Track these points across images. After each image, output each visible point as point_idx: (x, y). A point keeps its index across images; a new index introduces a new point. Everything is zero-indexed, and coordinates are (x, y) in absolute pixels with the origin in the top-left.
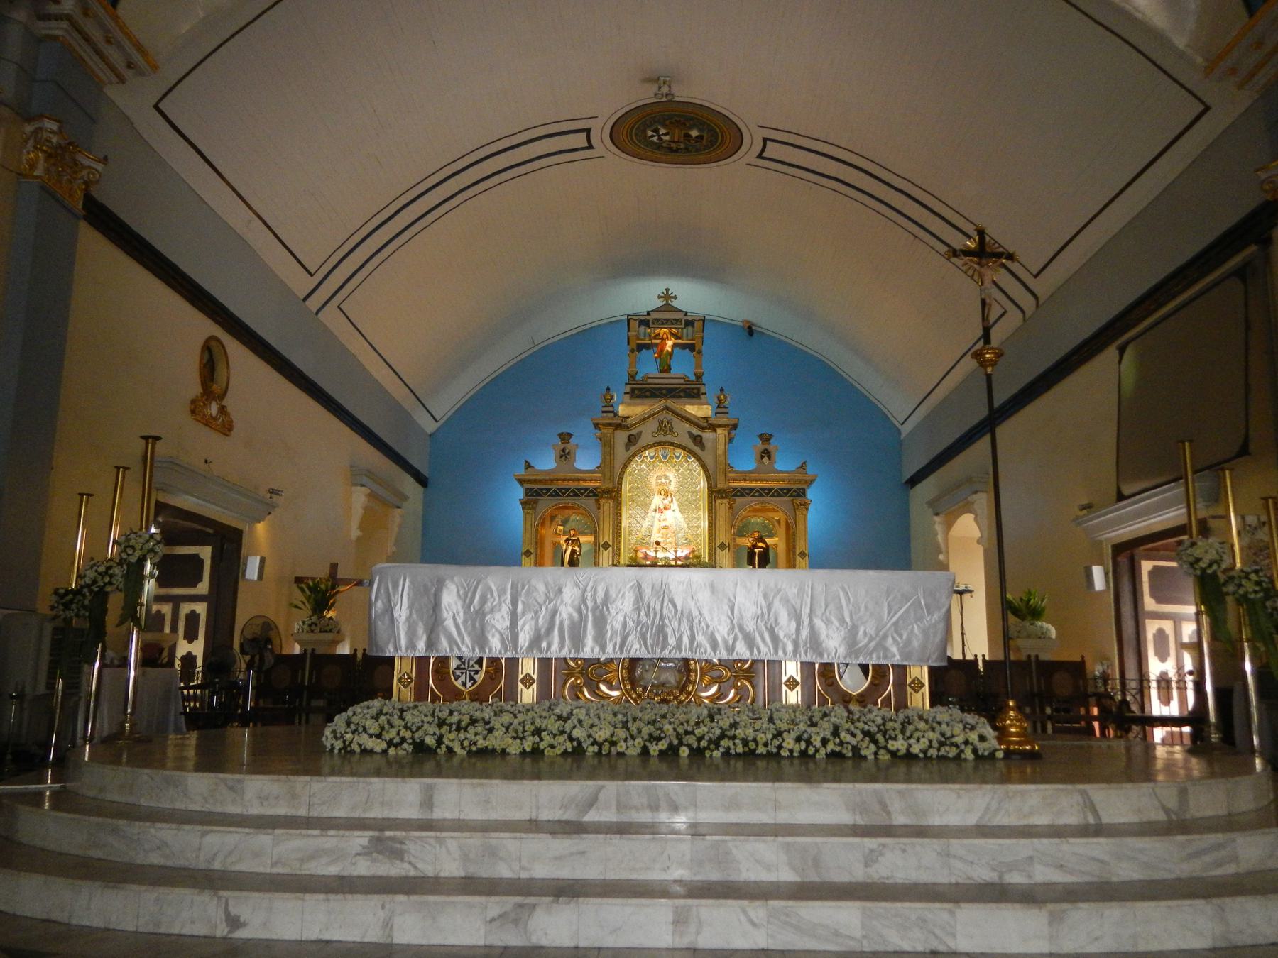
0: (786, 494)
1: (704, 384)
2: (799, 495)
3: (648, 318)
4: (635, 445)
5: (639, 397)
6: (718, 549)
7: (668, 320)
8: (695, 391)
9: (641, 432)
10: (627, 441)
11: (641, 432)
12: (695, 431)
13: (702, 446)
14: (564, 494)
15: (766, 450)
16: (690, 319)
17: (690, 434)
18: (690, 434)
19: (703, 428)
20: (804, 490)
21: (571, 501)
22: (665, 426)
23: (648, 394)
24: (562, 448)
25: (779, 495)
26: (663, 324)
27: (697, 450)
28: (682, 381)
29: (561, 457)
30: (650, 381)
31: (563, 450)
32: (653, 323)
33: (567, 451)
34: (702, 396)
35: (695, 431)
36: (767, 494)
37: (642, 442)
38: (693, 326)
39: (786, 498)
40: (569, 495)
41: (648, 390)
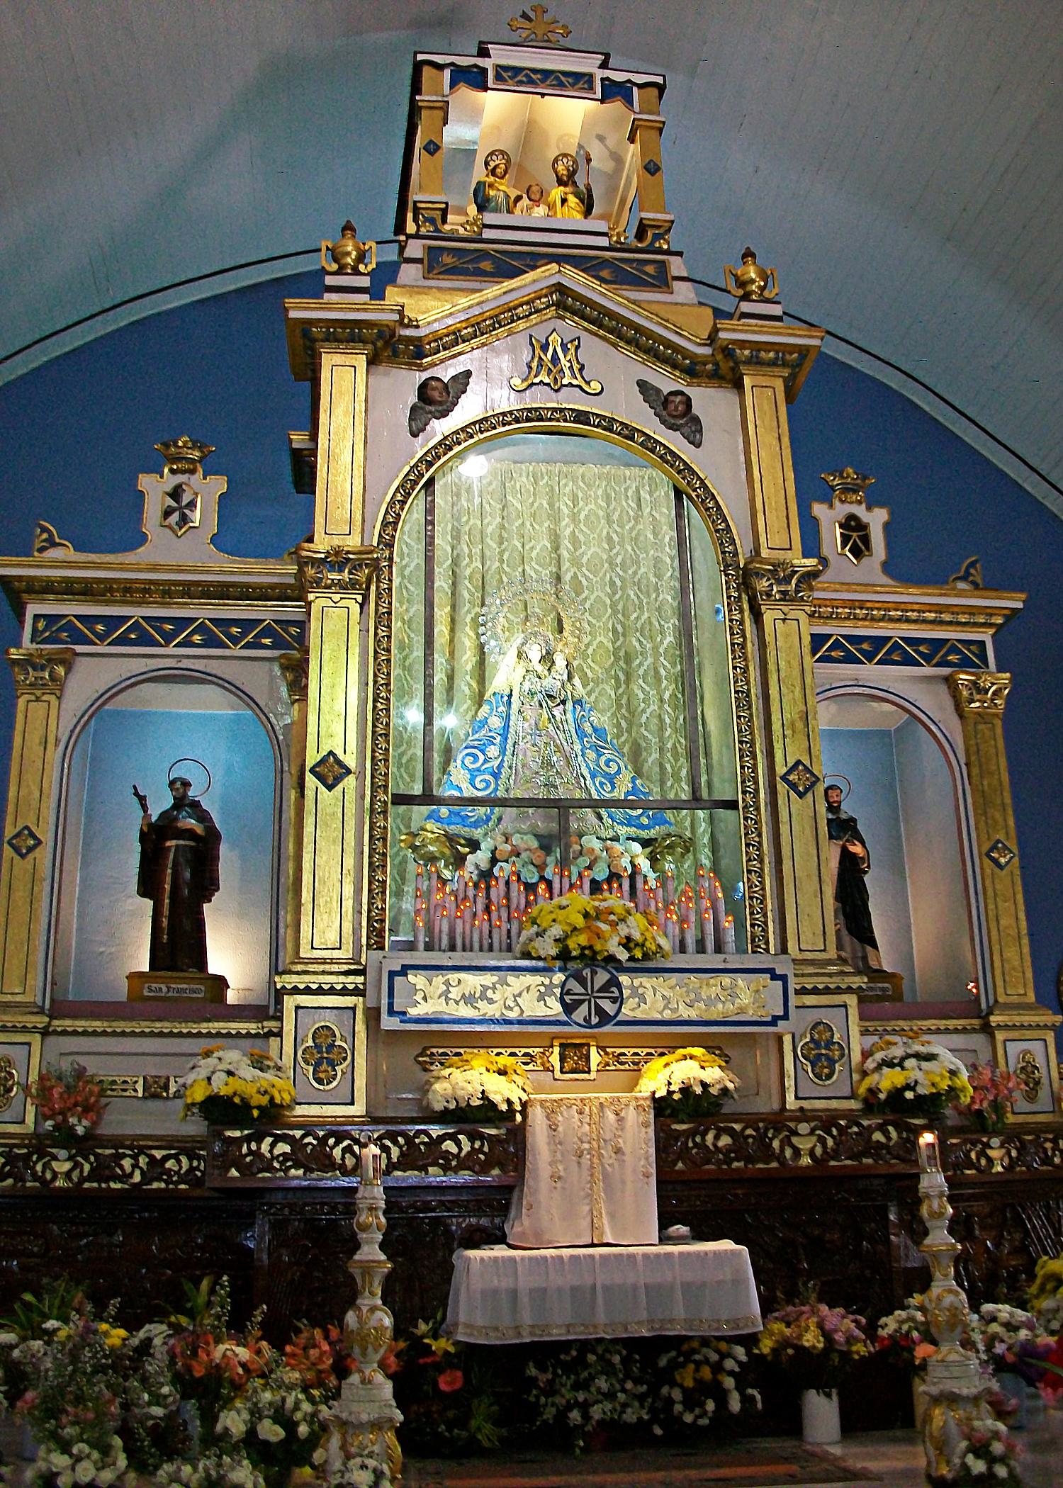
0: (928, 659)
1: (680, 254)
2: (965, 664)
3: (481, 62)
4: (444, 414)
5: (452, 271)
6: (782, 787)
7: (546, 74)
8: (650, 269)
9: (468, 374)
10: (413, 398)
11: (468, 374)
12: (666, 382)
13: (690, 425)
14: (168, 638)
15: (852, 517)
16: (618, 77)
17: (643, 386)
18: (643, 386)
19: (692, 370)
20: (982, 644)
21: (197, 658)
22: (555, 359)
23: (486, 265)
24: (169, 488)
25: (909, 661)
26: (531, 82)
27: (674, 441)
28: (603, 242)
29: (167, 513)
30: (487, 234)
31: (176, 493)
32: (498, 77)
33: (186, 499)
34: (677, 285)
35: (666, 382)
36: (870, 657)
37: (468, 409)
38: (629, 102)
39: (927, 670)
40: (187, 643)
41: (485, 255)
